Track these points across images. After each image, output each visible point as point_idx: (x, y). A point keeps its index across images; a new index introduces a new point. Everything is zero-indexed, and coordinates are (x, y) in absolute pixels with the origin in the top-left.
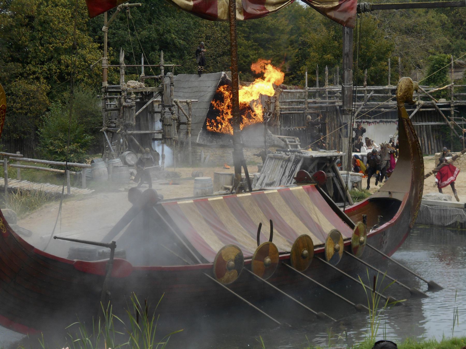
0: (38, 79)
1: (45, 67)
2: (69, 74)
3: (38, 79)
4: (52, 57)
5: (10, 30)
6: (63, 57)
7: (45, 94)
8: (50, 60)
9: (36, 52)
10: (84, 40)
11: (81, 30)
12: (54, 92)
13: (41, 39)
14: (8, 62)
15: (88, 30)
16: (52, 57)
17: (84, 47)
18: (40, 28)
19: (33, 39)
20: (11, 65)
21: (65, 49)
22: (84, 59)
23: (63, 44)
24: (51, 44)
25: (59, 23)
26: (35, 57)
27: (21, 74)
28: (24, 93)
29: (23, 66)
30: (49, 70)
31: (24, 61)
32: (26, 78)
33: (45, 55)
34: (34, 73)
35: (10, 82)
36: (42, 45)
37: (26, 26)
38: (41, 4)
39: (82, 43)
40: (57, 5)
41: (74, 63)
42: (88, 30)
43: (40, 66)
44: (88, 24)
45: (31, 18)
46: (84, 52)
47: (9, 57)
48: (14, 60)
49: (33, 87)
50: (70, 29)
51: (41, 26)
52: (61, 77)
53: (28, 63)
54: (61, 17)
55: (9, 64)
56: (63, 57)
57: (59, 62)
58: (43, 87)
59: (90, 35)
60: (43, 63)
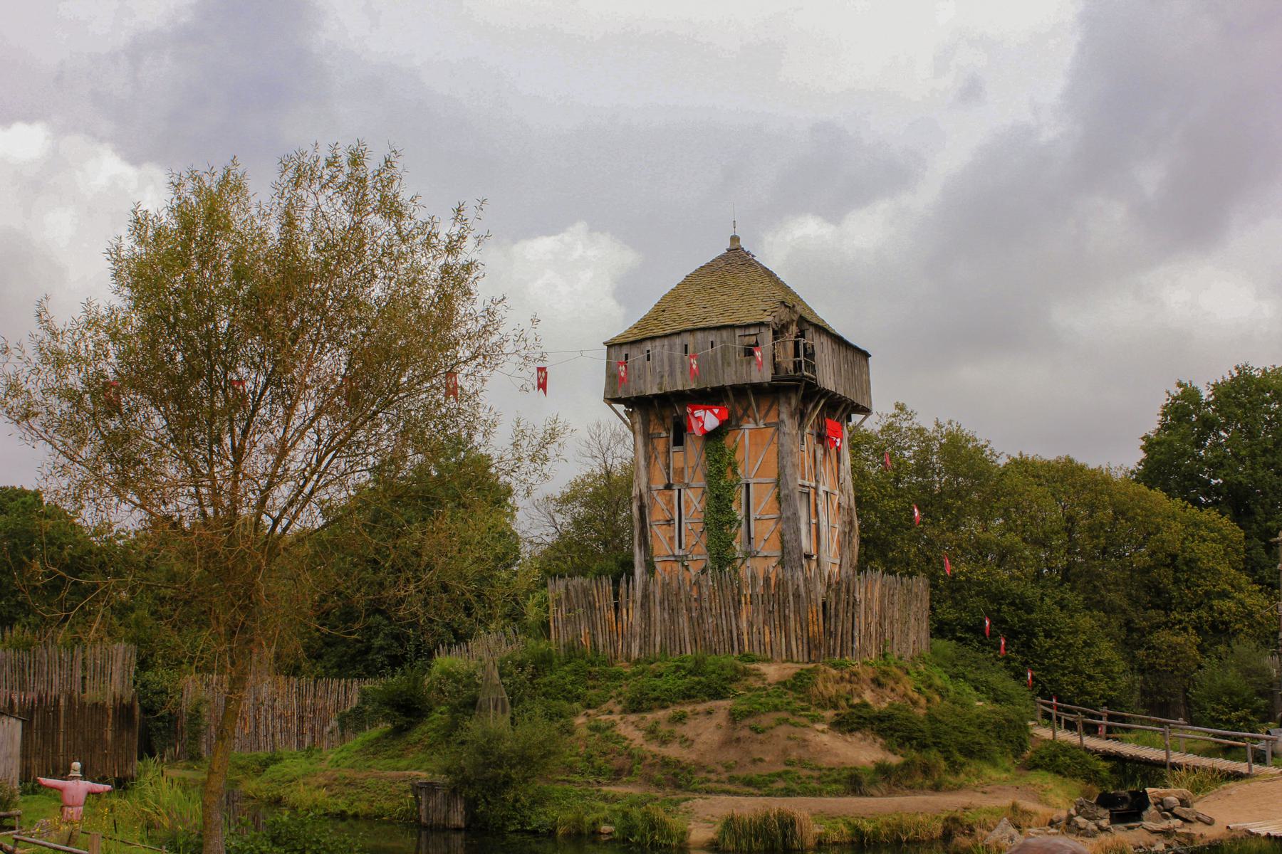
0: (1185, 629)
1: (1194, 615)
2: (1223, 623)
3: (1185, 629)
4: (1201, 603)
5: (1148, 572)
6: (1215, 602)
7: (1195, 647)
8: (1198, 606)
9: (1182, 597)
10: (1242, 581)
11: (1237, 569)
12: (1206, 645)
13: (1187, 581)
14: (1146, 609)
15: (1245, 569)
16: (1201, 603)
17: (1241, 590)
18: (1185, 568)
19: (1177, 581)
20: (1152, 613)
21: (1218, 592)
22: (1243, 604)
23: (1214, 586)
24: (1199, 586)
25: (1209, 561)
26: (1180, 603)
27: (1166, 624)
28: (1169, 646)
29: (1166, 613)
30: (1199, 618)
31: (1167, 607)
32: (1170, 628)
33: (1193, 600)
34: (1180, 622)
35: (1150, 633)
36: (1188, 588)
37: (1168, 566)
38: (1186, 539)
39: (1239, 584)
40: (1205, 540)
41: (1229, 609)
42: (1245, 569)
43: (1187, 614)
44: (1245, 561)
45: (1174, 557)
46: (1241, 596)
47: (1149, 603)
48: (1156, 607)
49: (1180, 639)
50: (1223, 568)
51: (1187, 565)
52: (1213, 626)
53: (1171, 610)
54: (1212, 554)
55: (1149, 611)
56: (1215, 602)
57: (1211, 608)
58: (1193, 638)
59: (1247, 575)
60: (1190, 610)
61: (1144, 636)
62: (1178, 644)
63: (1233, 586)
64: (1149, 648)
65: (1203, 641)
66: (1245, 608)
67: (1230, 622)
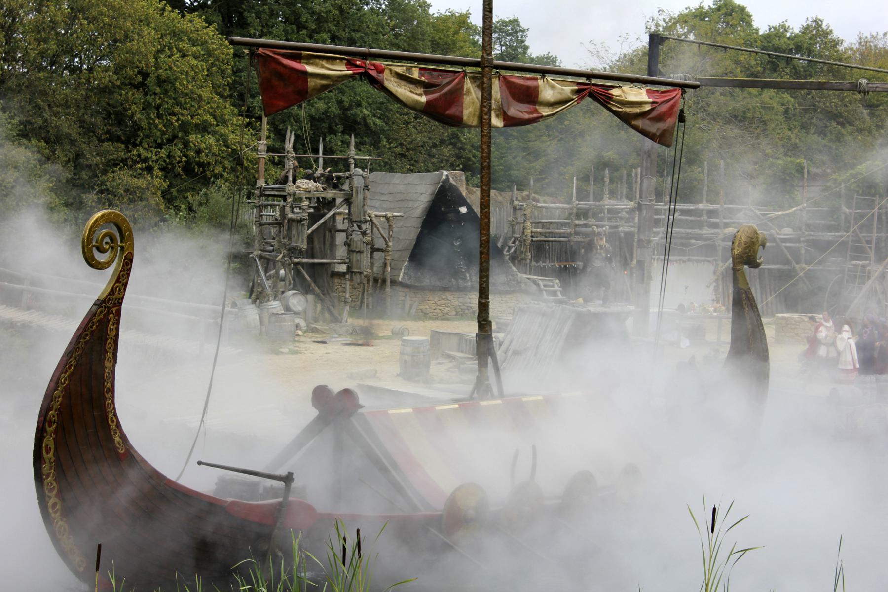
0: (149, 169)
1: (163, 153)
2: (201, 165)
3: (149, 169)
4: (175, 137)
5: (111, 92)
6: (192, 137)
7: (159, 193)
8: (170, 141)
9: (150, 129)
10: (226, 111)
11: (222, 96)
12: (174, 191)
13: (158, 107)
14: (103, 141)
15: (231, 96)
16: (175, 137)
17: (224, 123)
18: (158, 90)
19: (146, 106)
20: (108, 146)
21: (197, 125)
22: (225, 141)
23: (192, 117)
24: (174, 114)
25: (188, 82)
26: (148, 136)
27: (124, 161)
28: (126, 191)
29: (127, 147)
30: (169, 156)
31: (130, 141)
32: (130, 168)
33: (163, 133)
34: (146, 160)
35: (105, 172)
36: (159, 116)
37: (137, 87)
38: (159, 51)
39: (222, 116)
40: (184, 56)
41: (209, 148)
42: (231, 96)
43: (155, 151)
44: (232, 86)
45: (145, 75)
46: (222, 130)
47: (106, 133)
48: (114, 139)
49: (141, 183)
50: (205, 93)
51: (160, 86)
52: (188, 169)
53: (135, 145)
54: (192, 74)
55: (105, 144)
56: (192, 137)
57: (186, 144)
58: (157, 182)
59: (234, 105)
60: (160, 146)
61: (96, 176)
62: (138, 188)
63: (215, 118)
64: (101, 192)
65: (171, 186)
66: (227, 146)
67: (209, 164)
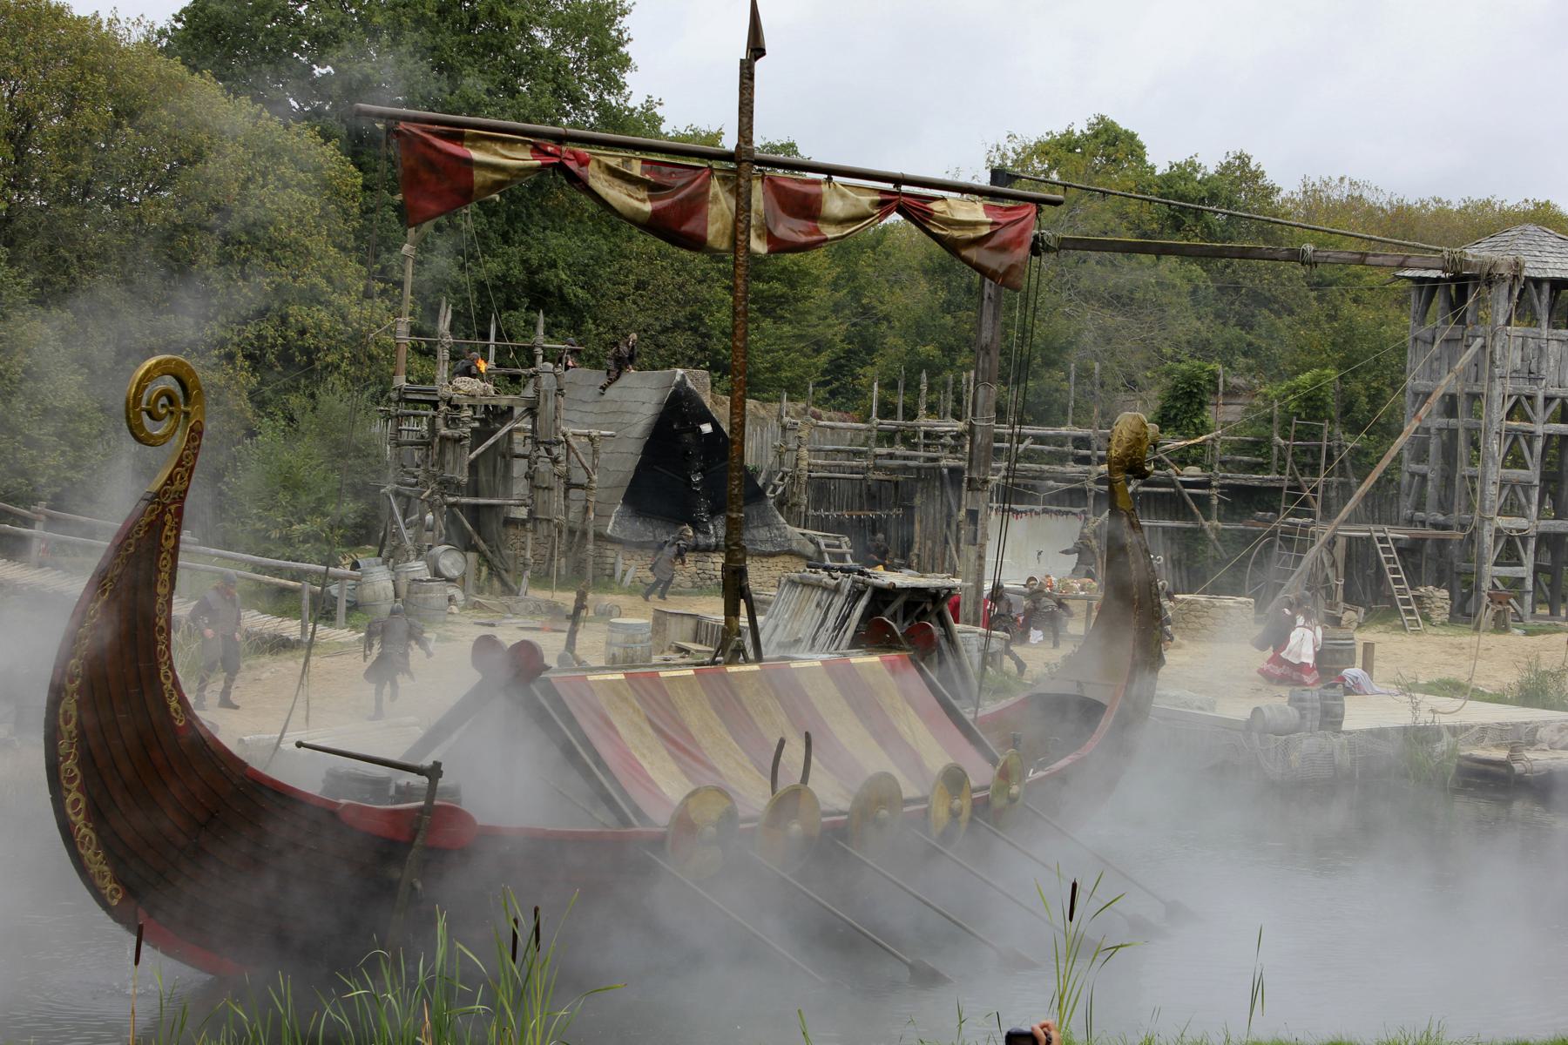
2: (306, 351)
7: (245, 395)
11: (343, 248)
15: (357, 249)
16: (268, 309)
17: (347, 290)
21: (301, 291)
22: (344, 318)
23: (295, 278)
25: (290, 227)
30: (259, 337)
38: (249, 179)
40: (286, 186)
41: (318, 326)
42: (357, 249)
43: (236, 328)
46: (344, 301)
50: (317, 244)
51: (248, 233)
57: (284, 320)
58: (243, 377)
59: (361, 262)
63: (330, 280)
65: (261, 383)
67: (318, 349)
